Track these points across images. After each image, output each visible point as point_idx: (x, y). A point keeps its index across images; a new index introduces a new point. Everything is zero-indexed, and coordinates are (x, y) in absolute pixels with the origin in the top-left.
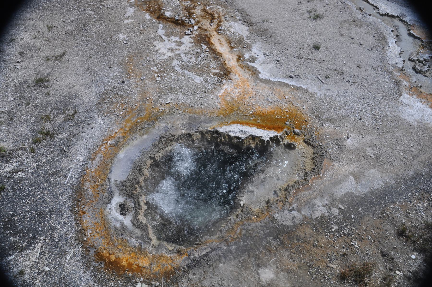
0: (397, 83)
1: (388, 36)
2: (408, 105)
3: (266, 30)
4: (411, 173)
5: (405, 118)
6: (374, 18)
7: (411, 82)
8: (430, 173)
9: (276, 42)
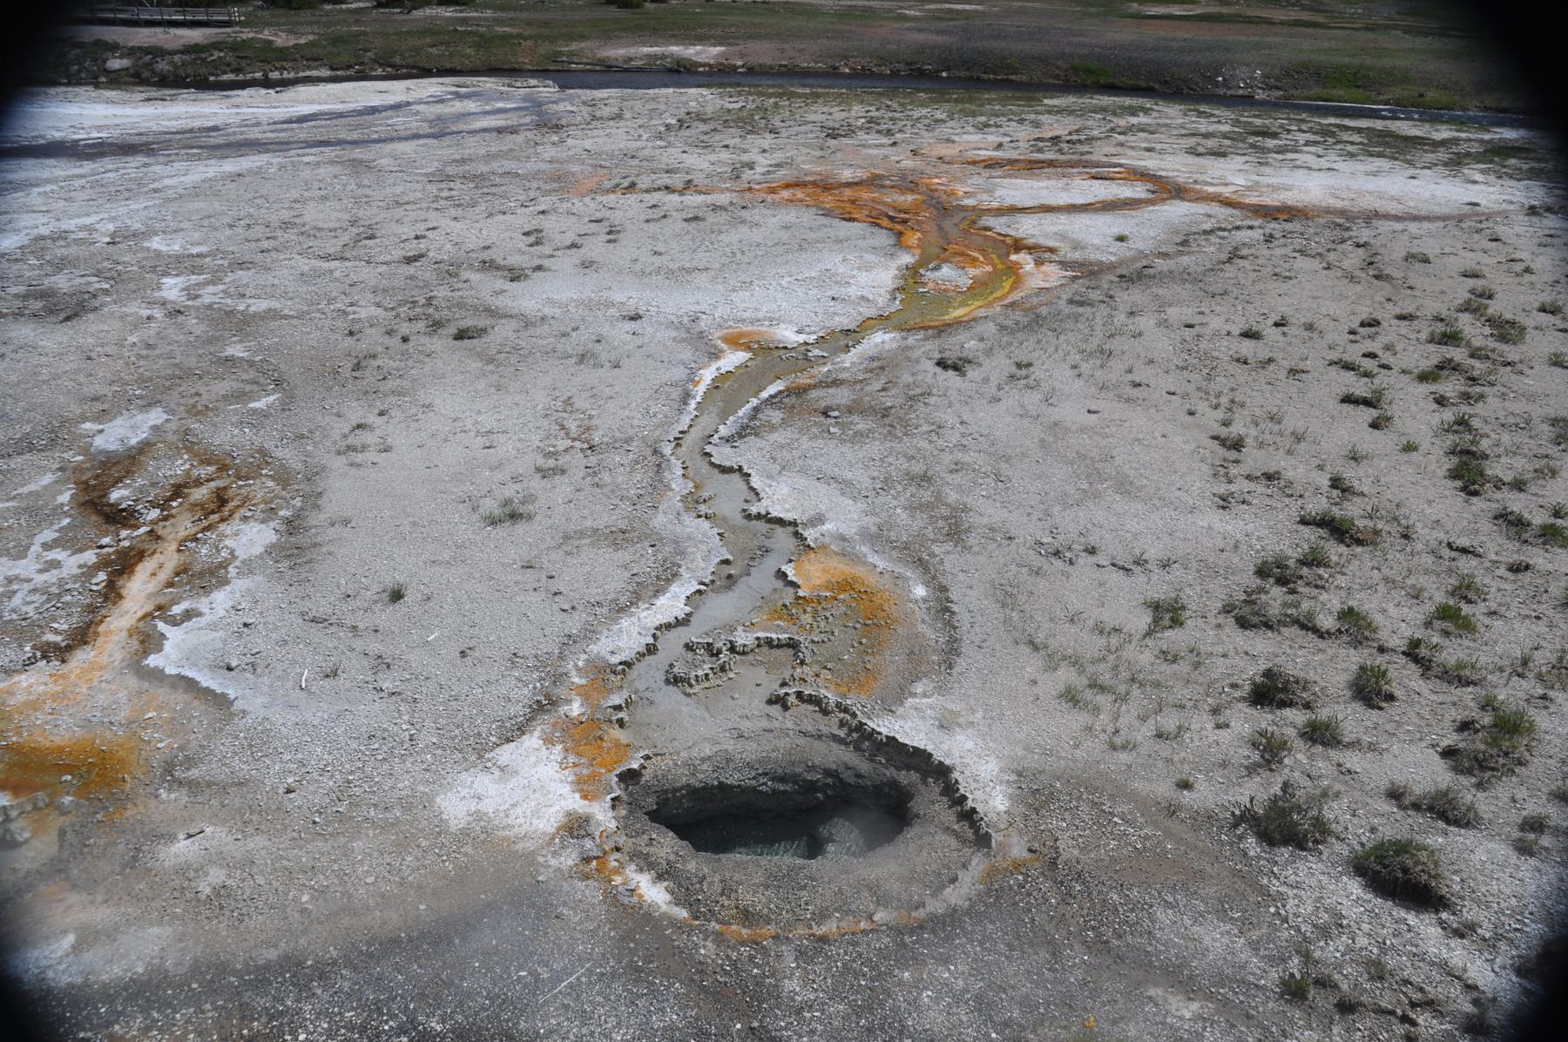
0: (544, 706)
1: (686, 575)
2: (502, 769)
3: (315, 545)
4: (273, 954)
5: (444, 804)
6: (706, 524)
7: (598, 706)
8: (335, 963)
9: (303, 576)
